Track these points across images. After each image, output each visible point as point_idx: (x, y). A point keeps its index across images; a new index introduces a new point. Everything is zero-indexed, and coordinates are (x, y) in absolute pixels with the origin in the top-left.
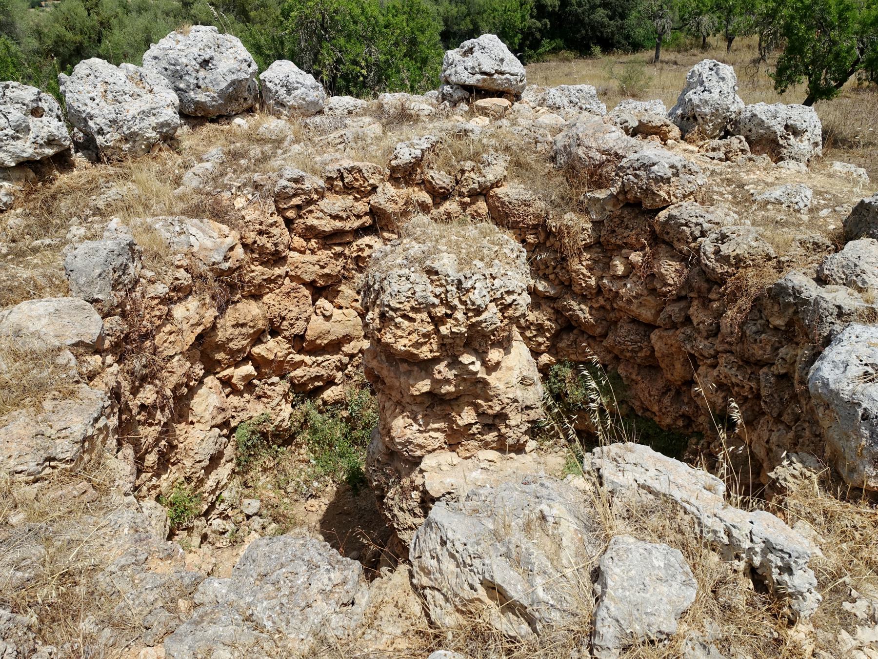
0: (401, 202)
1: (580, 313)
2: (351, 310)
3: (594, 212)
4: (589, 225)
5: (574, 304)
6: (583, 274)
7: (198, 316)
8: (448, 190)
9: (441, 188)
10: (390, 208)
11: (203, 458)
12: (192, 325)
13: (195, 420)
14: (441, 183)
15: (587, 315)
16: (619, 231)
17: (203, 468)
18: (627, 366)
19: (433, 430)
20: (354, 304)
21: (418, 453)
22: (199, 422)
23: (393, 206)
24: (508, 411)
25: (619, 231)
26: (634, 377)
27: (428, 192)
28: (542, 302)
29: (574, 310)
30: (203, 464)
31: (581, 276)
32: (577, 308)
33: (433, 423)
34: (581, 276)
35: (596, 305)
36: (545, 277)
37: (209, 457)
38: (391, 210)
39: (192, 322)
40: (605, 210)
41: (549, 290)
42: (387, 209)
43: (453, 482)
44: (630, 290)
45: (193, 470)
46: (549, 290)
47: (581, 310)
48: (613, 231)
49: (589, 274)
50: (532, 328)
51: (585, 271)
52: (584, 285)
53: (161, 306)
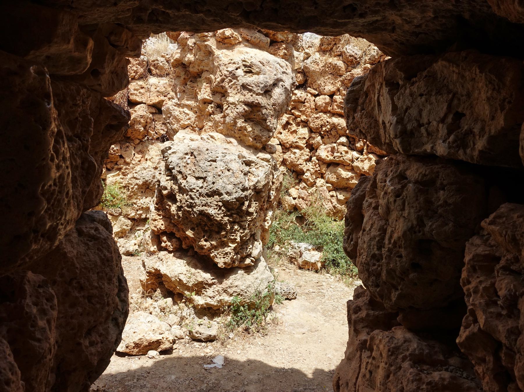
0: (321, 65)
2: (276, 139)
7: (164, 89)
8: (356, 58)
9: (350, 56)
10: (313, 67)
11: (139, 177)
12: (158, 91)
13: (148, 159)
14: (351, 52)
17: (137, 184)
19: (188, 106)
20: (279, 135)
21: (175, 126)
22: (150, 160)
23: (316, 66)
24: (226, 85)
27: (344, 62)
30: (138, 181)
33: (187, 100)
37: (144, 180)
38: (313, 69)
39: (158, 89)
42: (310, 67)
45: (130, 182)
53: (138, 66)
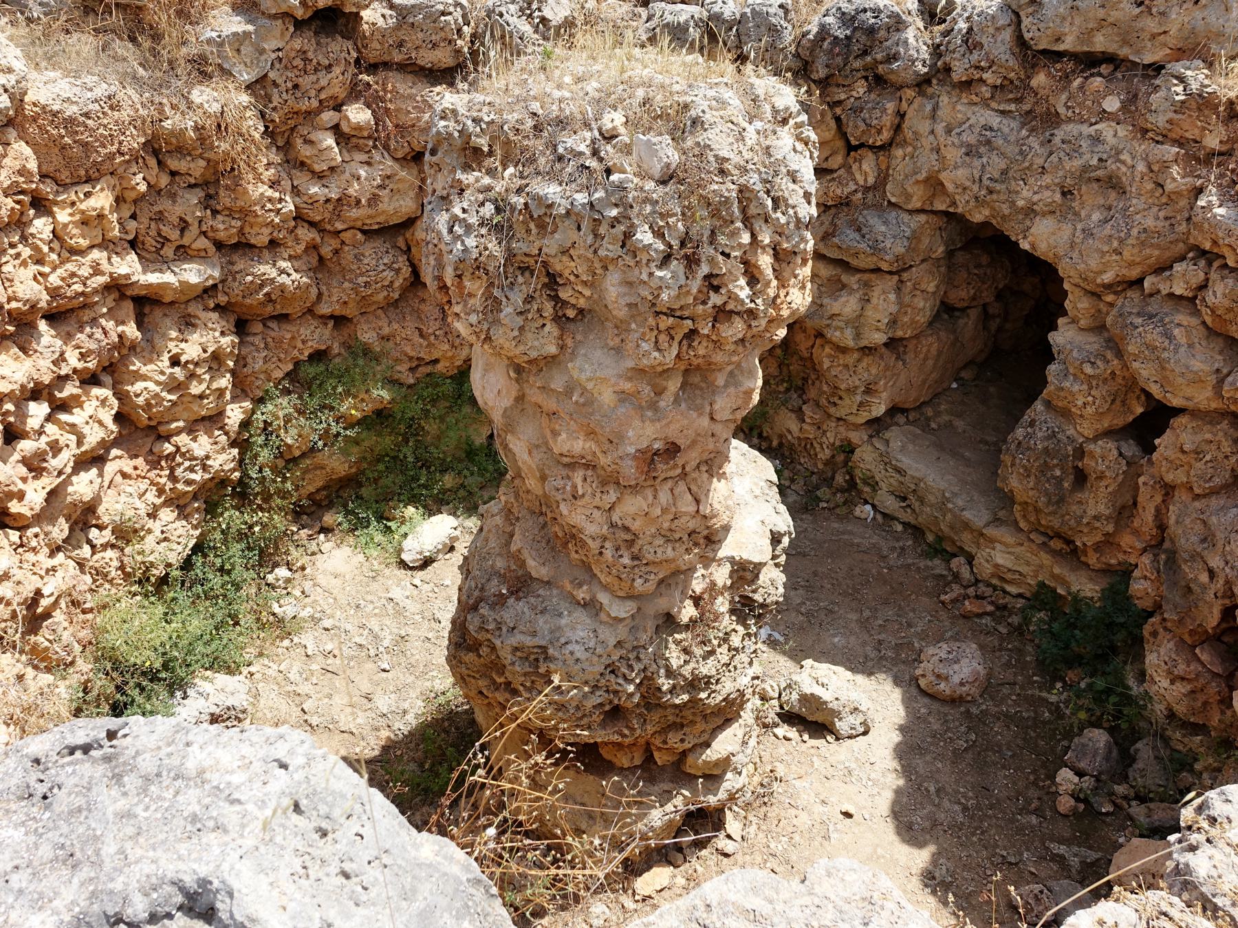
1: (283, 279)
3: (242, 67)
4: (245, 98)
5: (266, 270)
6: (270, 200)
15: (295, 276)
16: (305, 81)
18: (367, 322)
25: (305, 81)
26: (386, 331)
28: (193, 309)
29: (273, 280)
31: (269, 206)
32: (273, 273)
34: (269, 206)
35: (300, 249)
36: (184, 253)
40: (262, 52)
41: (209, 272)
43: (759, 518)
44: (370, 178)
46: (209, 272)
47: (282, 272)
48: (296, 86)
49: (277, 195)
50: (199, 371)
51: (270, 193)
52: (277, 220)
